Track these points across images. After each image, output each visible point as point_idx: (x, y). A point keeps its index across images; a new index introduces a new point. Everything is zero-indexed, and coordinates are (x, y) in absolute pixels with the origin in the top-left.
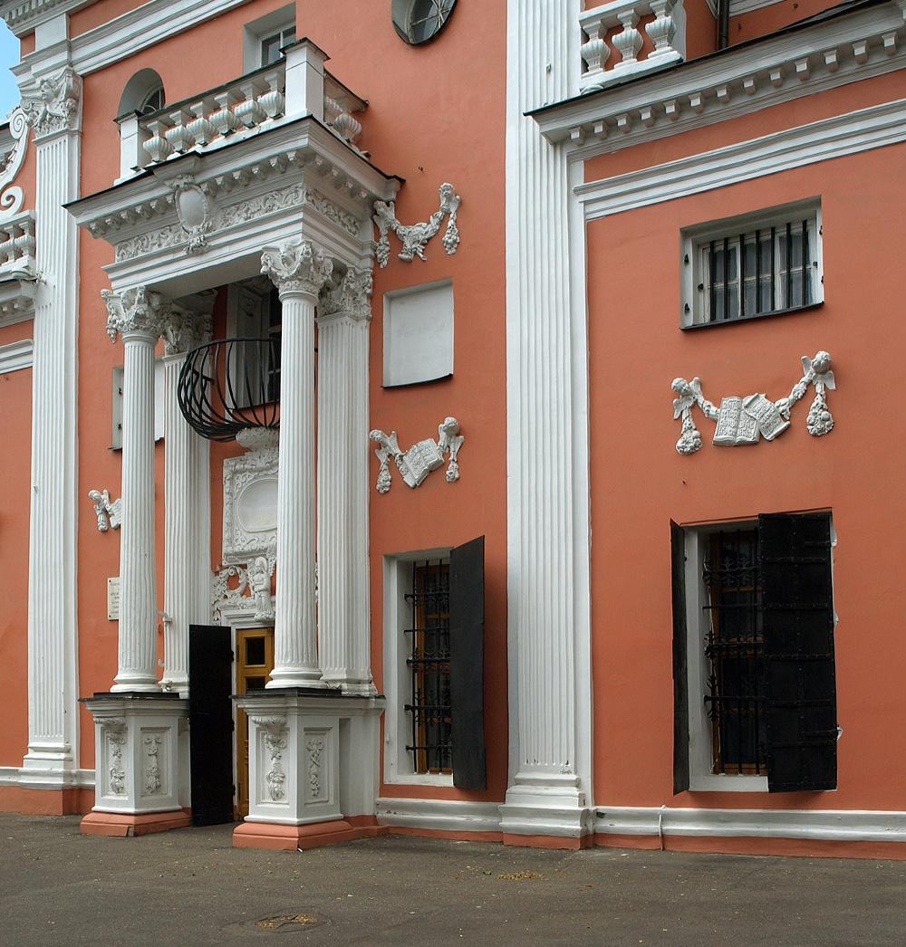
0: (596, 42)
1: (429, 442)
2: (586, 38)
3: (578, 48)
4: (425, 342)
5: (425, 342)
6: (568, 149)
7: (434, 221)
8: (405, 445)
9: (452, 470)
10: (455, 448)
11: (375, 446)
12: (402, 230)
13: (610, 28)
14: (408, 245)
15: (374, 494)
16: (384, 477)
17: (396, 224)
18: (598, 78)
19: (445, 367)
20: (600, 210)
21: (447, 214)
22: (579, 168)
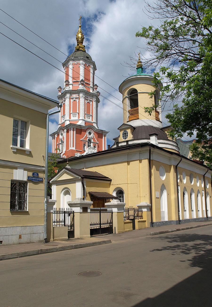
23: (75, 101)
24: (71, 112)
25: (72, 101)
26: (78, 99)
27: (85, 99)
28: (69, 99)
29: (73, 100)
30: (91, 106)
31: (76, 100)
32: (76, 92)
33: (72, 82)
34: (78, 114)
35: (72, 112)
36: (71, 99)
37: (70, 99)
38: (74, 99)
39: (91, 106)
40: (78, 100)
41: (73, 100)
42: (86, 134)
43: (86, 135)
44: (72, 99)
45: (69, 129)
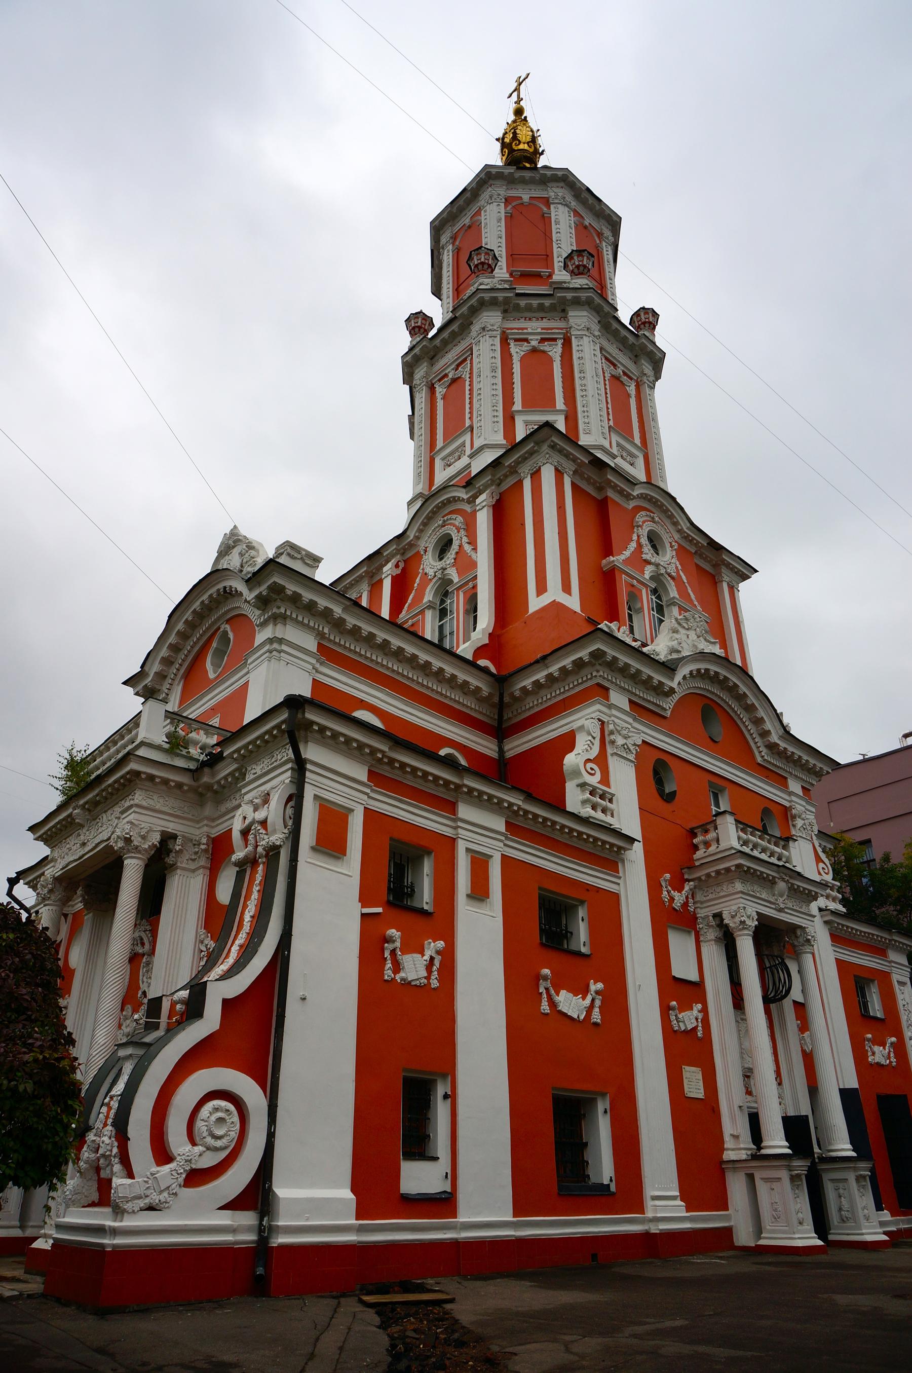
23: (534, 350)
24: (518, 406)
25: (517, 351)
26: (560, 342)
29: (526, 347)
30: (633, 402)
31: (545, 347)
32: (541, 308)
33: (508, 275)
35: (520, 408)
38: (534, 343)
39: (633, 402)
41: (526, 347)
42: (635, 537)
43: (633, 545)
44: (516, 340)
45: (520, 483)
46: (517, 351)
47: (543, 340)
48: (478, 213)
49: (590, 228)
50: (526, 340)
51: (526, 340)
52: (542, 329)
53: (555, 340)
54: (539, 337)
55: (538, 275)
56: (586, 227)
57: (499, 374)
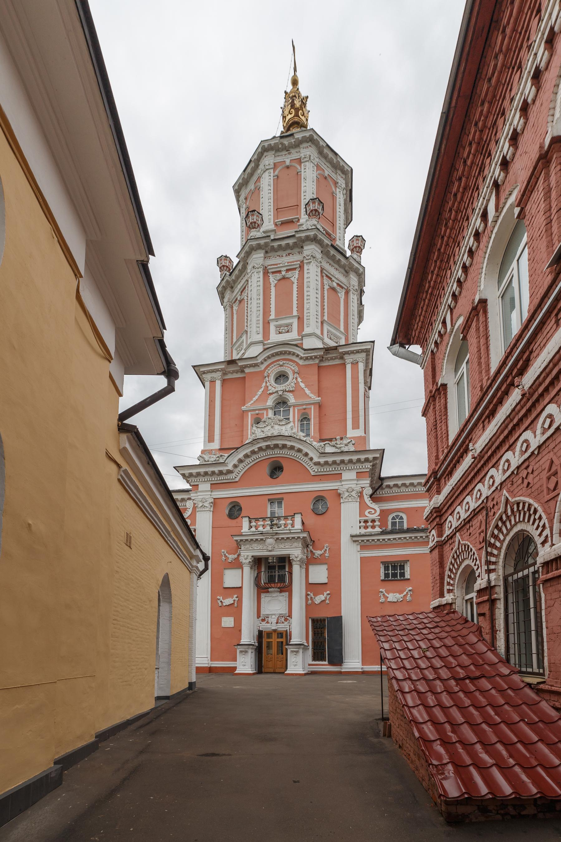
0: (362, 524)
1: (322, 595)
2: (360, 522)
3: (359, 525)
4: (319, 574)
5: (319, 574)
6: (357, 543)
7: (323, 551)
8: (315, 595)
9: (327, 601)
10: (328, 597)
11: (307, 595)
12: (314, 551)
13: (366, 522)
14: (316, 554)
15: (307, 605)
16: (310, 602)
17: (313, 550)
18: (363, 531)
19: (326, 581)
20: (362, 555)
21: (326, 550)
22: (359, 547)
23: (284, 278)
27: (321, 272)
28: (261, 274)
29: (279, 276)
31: (289, 274)
33: (273, 226)
34: (300, 319)
36: (271, 275)
37: (266, 273)
40: (294, 276)
41: (279, 276)
44: (273, 273)
46: (272, 279)
47: (288, 270)
48: (259, 178)
49: (328, 178)
50: (280, 272)
51: (280, 272)
52: (288, 263)
53: (295, 269)
54: (285, 269)
55: (291, 222)
56: (326, 178)
57: (261, 297)
